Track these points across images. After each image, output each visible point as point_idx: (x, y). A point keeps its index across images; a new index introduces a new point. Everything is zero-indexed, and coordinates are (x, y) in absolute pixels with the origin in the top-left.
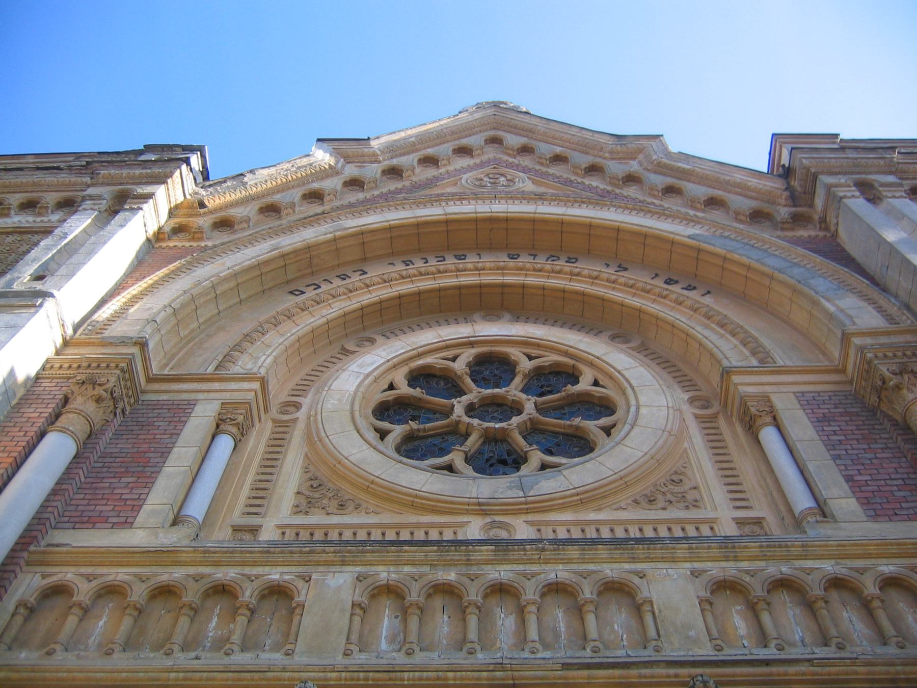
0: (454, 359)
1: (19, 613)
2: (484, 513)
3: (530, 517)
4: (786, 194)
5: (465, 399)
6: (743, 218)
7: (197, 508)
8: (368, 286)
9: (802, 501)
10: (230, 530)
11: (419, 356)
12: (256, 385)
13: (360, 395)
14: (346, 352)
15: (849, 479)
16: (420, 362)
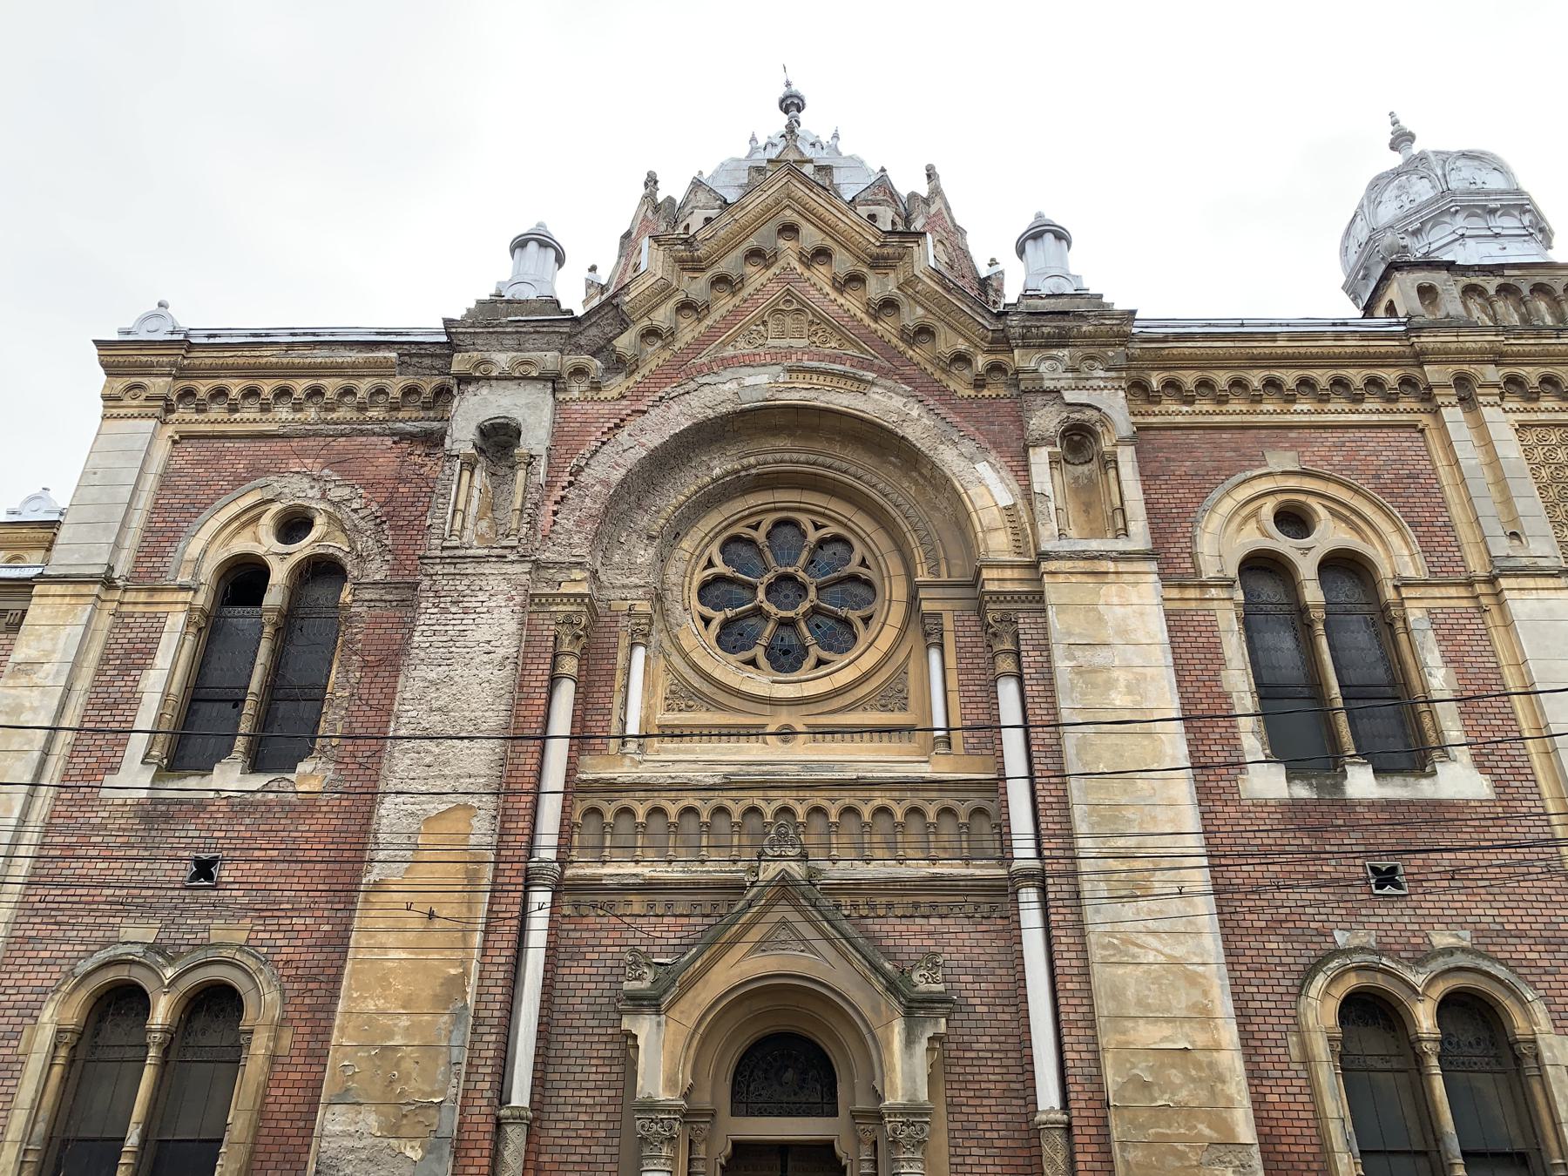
0: (756, 527)
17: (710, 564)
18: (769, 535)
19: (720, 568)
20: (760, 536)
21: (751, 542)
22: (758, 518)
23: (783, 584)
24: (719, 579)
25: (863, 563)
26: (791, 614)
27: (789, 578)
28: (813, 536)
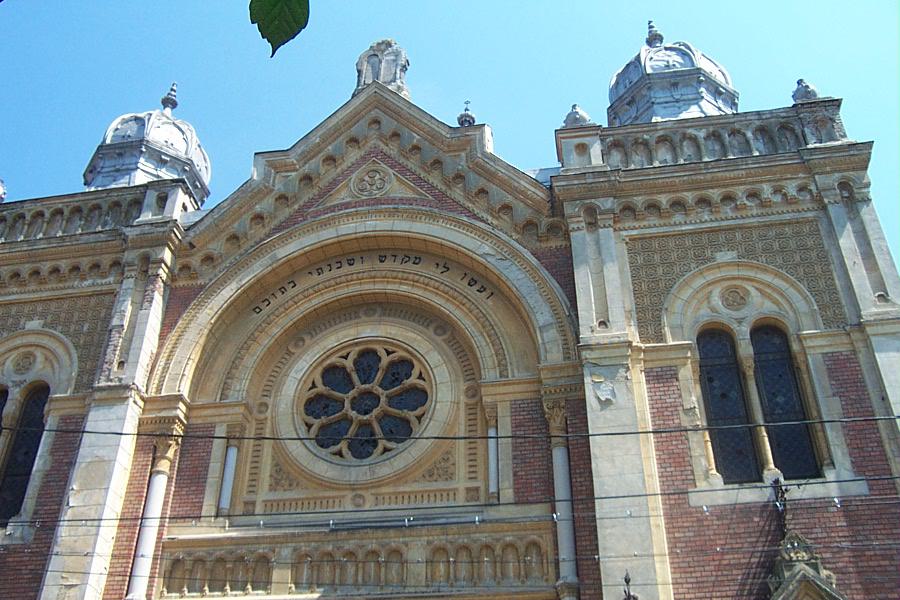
0: (346, 357)
1: (159, 472)
2: (354, 490)
3: (373, 491)
4: (549, 205)
5: (352, 393)
7: (225, 504)
8: (296, 303)
9: (493, 489)
10: (243, 504)
11: (328, 357)
12: (241, 410)
14: (290, 353)
15: (515, 474)
16: (328, 362)
17: (314, 385)
18: (355, 363)
19: (321, 388)
20: (349, 364)
21: (344, 368)
22: (348, 350)
23: (365, 397)
24: (320, 397)
25: (420, 377)
26: (365, 418)
27: (369, 393)
28: (385, 360)
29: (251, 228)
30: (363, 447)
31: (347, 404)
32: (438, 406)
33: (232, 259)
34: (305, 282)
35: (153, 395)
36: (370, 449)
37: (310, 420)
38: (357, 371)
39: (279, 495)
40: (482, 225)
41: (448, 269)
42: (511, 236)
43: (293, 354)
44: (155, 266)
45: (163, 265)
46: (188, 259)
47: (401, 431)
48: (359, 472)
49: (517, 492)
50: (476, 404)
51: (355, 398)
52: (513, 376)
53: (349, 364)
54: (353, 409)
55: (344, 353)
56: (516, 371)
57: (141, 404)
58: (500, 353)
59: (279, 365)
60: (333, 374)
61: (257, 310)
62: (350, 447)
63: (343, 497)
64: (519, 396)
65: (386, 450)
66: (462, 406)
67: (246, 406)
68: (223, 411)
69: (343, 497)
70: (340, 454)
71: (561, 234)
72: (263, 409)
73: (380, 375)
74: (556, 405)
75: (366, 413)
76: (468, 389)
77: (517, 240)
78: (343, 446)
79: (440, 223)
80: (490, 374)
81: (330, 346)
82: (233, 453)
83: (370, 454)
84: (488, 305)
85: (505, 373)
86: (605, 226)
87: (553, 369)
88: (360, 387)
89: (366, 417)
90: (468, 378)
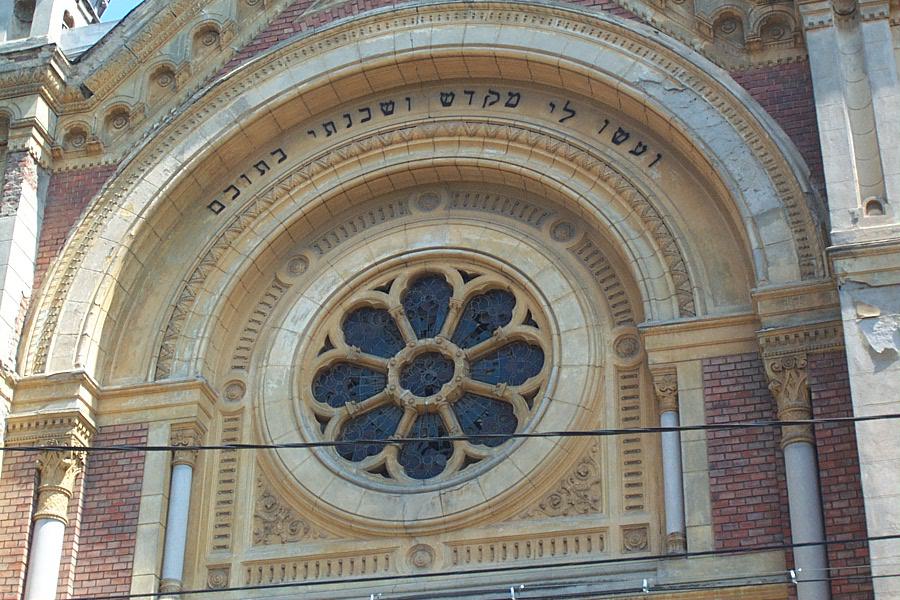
0: (386, 289)
1: (48, 518)
2: (411, 536)
3: (449, 537)
5: (401, 357)
6: (706, 32)
7: (174, 571)
9: (673, 526)
10: (207, 570)
11: (352, 290)
12: (195, 395)
13: (296, 370)
14: (280, 286)
15: (715, 498)
16: (354, 299)
17: (329, 345)
18: (405, 299)
19: (342, 349)
20: (393, 301)
21: (382, 311)
24: (341, 365)
25: (529, 320)
27: (433, 355)
28: (461, 291)
29: (196, 53)
30: (426, 455)
31: (393, 378)
32: (564, 375)
33: (163, 113)
34: (303, 151)
35: (30, 374)
36: (439, 458)
37: (325, 409)
38: (409, 314)
39: (273, 551)
40: (634, 25)
41: (573, 113)
42: (692, 45)
43: (288, 286)
44: (18, 133)
45: (34, 131)
46: (80, 117)
47: (495, 424)
48: (420, 503)
49: (719, 531)
50: (636, 368)
51: (405, 365)
52: (706, 313)
53: (393, 301)
54: (404, 385)
55: (382, 281)
56: (709, 302)
57: (9, 392)
58: (678, 271)
59: (262, 308)
60: (364, 322)
61: (215, 207)
62: (401, 457)
63: (392, 550)
64: (717, 351)
65: (469, 460)
66: (610, 372)
67: (204, 388)
68: (161, 399)
69: (392, 550)
70: (383, 470)
71: (788, 35)
72: (236, 392)
73: (451, 321)
74: (787, 365)
75: (429, 392)
76: (619, 341)
77: (702, 52)
78: (388, 455)
79: (554, 25)
80: (660, 309)
81: (355, 270)
82: (183, 475)
83: (438, 469)
84: (653, 179)
85: (688, 307)
86: (873, 18)
87: (779, 296)
88: (415, 343)
89: (429, 400)
90: (619, 319)
